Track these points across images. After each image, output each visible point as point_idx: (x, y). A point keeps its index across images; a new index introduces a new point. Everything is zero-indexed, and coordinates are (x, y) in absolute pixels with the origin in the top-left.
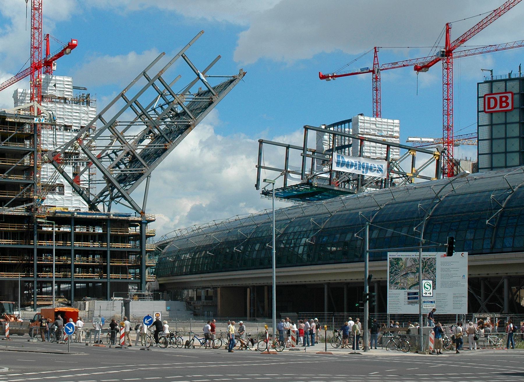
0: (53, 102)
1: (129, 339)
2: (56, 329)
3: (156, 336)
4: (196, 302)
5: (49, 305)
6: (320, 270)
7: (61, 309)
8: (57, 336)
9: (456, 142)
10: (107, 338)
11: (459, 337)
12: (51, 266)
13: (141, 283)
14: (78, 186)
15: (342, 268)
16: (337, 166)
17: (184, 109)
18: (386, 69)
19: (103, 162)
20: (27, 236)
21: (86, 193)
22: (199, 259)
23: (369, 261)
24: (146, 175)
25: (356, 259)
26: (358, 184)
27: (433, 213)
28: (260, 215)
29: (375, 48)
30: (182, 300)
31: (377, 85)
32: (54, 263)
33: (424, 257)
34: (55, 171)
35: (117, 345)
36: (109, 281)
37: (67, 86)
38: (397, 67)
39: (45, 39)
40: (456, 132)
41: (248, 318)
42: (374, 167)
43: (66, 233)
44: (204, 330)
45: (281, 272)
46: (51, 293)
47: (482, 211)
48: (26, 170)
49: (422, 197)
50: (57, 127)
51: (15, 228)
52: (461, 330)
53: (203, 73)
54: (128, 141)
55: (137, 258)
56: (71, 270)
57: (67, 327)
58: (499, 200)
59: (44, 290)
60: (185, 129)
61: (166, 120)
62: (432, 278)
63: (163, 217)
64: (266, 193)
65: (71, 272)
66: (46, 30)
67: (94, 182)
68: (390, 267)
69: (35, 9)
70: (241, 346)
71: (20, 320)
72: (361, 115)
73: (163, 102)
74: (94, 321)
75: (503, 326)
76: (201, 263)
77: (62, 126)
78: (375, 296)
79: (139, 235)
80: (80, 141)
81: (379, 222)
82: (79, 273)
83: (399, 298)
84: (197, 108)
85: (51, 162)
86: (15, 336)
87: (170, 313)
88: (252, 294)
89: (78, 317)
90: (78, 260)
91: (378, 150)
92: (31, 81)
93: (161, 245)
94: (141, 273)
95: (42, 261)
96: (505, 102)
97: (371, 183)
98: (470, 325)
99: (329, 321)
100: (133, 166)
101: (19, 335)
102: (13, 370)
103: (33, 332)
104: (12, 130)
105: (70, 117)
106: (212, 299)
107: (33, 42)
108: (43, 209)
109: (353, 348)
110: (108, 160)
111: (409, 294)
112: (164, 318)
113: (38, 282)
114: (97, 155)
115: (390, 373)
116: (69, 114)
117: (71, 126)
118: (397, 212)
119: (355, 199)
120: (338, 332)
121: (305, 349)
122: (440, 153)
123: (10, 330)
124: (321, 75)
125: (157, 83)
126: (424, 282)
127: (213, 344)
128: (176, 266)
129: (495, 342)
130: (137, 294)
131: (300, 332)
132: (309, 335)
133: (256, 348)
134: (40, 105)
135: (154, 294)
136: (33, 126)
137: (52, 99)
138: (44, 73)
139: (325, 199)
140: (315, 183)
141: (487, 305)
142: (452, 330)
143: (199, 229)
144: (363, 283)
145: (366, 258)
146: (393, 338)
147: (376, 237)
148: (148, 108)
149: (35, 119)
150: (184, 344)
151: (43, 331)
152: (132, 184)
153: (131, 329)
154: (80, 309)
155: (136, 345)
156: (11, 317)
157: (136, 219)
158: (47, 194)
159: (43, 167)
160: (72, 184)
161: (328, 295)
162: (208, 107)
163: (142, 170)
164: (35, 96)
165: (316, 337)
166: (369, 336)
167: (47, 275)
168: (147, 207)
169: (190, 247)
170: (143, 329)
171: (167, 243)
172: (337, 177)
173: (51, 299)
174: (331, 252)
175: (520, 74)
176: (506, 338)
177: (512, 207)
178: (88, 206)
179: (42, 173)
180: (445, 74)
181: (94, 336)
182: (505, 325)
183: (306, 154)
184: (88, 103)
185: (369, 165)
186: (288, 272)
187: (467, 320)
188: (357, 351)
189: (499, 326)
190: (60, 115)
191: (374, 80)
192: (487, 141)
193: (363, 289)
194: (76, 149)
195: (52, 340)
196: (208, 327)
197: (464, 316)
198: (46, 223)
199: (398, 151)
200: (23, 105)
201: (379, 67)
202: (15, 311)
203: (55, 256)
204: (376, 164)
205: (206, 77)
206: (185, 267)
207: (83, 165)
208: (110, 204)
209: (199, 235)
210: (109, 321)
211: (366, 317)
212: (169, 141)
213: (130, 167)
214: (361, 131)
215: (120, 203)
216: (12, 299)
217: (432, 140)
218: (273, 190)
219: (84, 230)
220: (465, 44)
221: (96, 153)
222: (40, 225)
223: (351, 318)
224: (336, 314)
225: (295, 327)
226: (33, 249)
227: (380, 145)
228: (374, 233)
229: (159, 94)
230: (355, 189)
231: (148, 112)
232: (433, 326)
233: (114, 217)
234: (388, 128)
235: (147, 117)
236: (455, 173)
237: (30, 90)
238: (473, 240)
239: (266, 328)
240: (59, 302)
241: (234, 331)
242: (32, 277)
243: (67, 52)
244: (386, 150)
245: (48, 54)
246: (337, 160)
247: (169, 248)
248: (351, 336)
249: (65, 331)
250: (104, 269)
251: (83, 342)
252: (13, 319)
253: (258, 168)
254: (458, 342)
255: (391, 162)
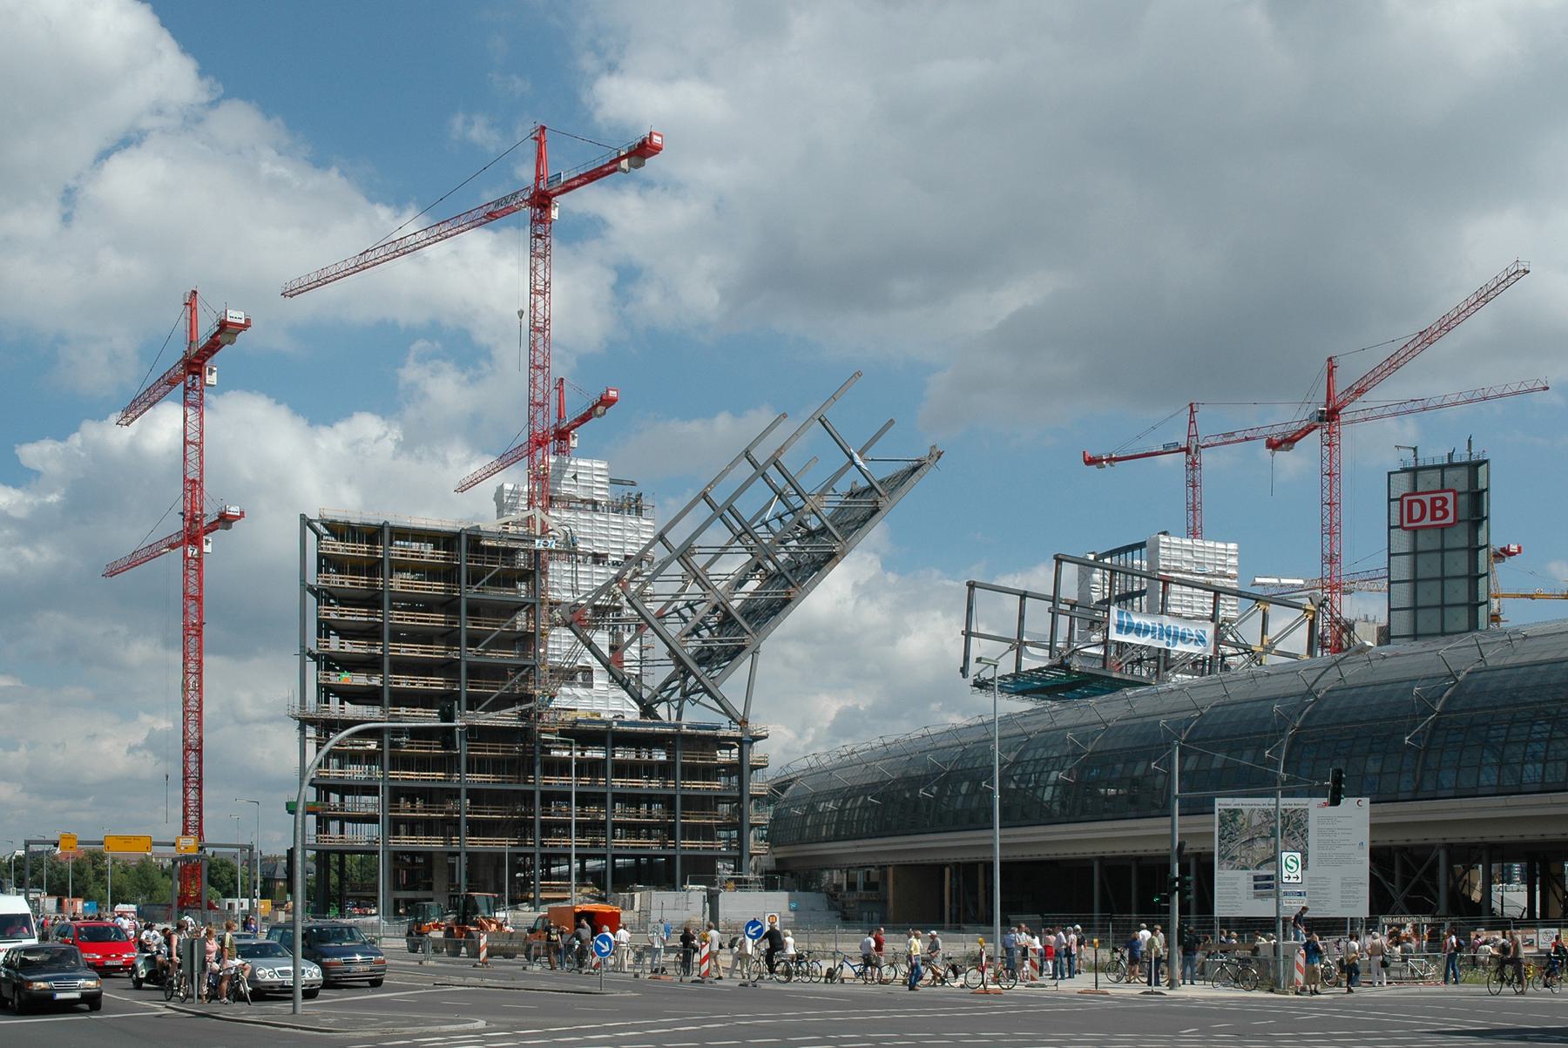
0: (571, 508)
1: (717, 966)
2: (576, 947)
3: (769, 960)
4: (847, 895)
5: (564, 900)
6: (1084, 832)
7: (587, 907)
8: (578, 959)
9: (1346, 586)
10: (676, 963)
11: (1352, 962)
12: (567, 825)
13: (741, 857)
14: (620, 670)
15: (1127, 829)
16: (1117, 632)
17: (822, 522)
18: (1213, 445)
19: (667, 625)
20: (521, 766)
21: (634, 684)
22: (852, 812)
23: (1180, 815)
24: (750, 649)
25: (1155, 811)
26: (1158, 668)
27: (1303, 721)
28: (970, 727)
29: (1191, 405)
30: (819, 890)
31: (1194, 477)
32: (574, 819)
33: (1285, 807)
34: (576, 642)
35: (695, 976)
36: (678, 854)
37: (599, 479)
38: (1233, 442)
39: (555, 388)
40: (1346, 566)
41: (947, 925)
42: (1189, 635)
43: (597, 760)
44: (861, 948)
45: (1009, 836)
46: (568, 877)
47: (1397, 718)
48: (519, 639)
49: (1281, 692)
50: (580, 557)
51: (498, 751)
52: (1357, 948)
53: (860, 454)
54: (715, 583)
55: (734, 810)
56: (606, 832)
57: (598, 942)
58: (1430, 698)
59: (554, 870)
60: (826, 562)
61: (788, 544)
62: (1301, 847)
63: (783, 730)
64: (981, 685)
65: (606, 836)
66: (557, 370)
67: (651, 663)
68: (1220, 827)
69: (538, 330)
70: (934, 978)
71: (508, 928)
72: (1165, 533)
73: (783, 509)
74: (649, 930)
75: (1438, 941)
76: (855, 818)
77: (589, 555)
78: (1192, 883)
79: (737, 764)
80: (623, 583)
81: (1199, 740)
82: (621, 838)
83: (1236, 886)
84: (849, 521)
85: (569, 625)
86: (499, 959)
87: (796, 915)
88: (954, 879)
89: (619, 922)
90: (620, 813)
91: (1197, 602)
92: (529, 468)
93: (779, 783)
94: (740, 838)
95: (550, 815)
96: (1439, 508)
97: (1184, 664)
98: (1375, 938)
99: (1103, 931)
100: (725, 632)
101: (506, 958)
102: (494, 1025)
103: (533, 952)
104: (492, 563)
105: (604, 538)
106: (877, 889)
107: (534, 393)
108: (552, 716)
109: (1149, 983)
110: (678, 620)
111: (1256, 878)
112: (785, 925)
113: (543, 856)
114: (656, 611)
115: (1221, 1031)
116: (603, 532)
117: (605, 556)
118: (1233, 720)
119: (1151, 695)
120: (1120, 952)
121: (1056, 985)
122: (1315, 607)
123: (488, 948)
124: (1086, 457)
125: (772, 471)
126: (1285, 855)
127: (878, 974)
128: (808, 824)
129: (1421, 971)
130: (733, 879)
131: (1047, 953)
132: (1065, 957)
133: (963, 983)
134: (547, 514)
135: (766, 878)
136: (533, 555)
137: (570, 503)
138: (554, 454)
139: (1095, 695)
140: (1076, 664)
141: (1407, 901)
142: (1339, 949)
143: (852, 753)
144: (1168, 857)
145: (1174, 811)
146: (1226, 963)
147: (1193, 769)
148: (754, 519)
149: (537, 541)
150: (824, 974)
151: (552, 950)
152: (724, 667)
153: (721, 947)
154: (623, 908)
155: (731, 977)
156: (490, 922)
157: (732, 734)
158: (560, 686)
159: (552, 633)
160: (607, 666)
161: (1102, 883)
162: (870, 518)
163: (743, 641)
164: (537, 498)
165: (1076, 962)
166: (1179, 958)
167: (560, 842)
168: (752, 711)
169: (836, 787)
170: (745, 946)
171: (791, 780)
172: (1117, 653)
173: (567, 889)
174: (1107, 798)
175: (1471, 454)
176: (1442, 964)
177: (1455, 712)
178: (638, 709)
179: (550, 646)
180: (1326, 454)
181: (650, 959)
182: (1441, 938)
183: (1059, 609)
184: (639, 511)
185: (1180, 631)
186: (1025, 835)
187: (1367, 928)
188: (1156, 989)
189: (1429, 941)
190: (585, 534)
191: (1190, 467)
192: (1407, 584)
193: (1167, 868)
194: (615, 599)
195: (571, 968)
196: (870, 942)
197: (1362, 921)
198: (557, 743)
199: (1234, 603)
200: (513, 514)
201: (1198, 441)
202: (498, 911)
203: (576, 805)
204: (1193, 629)
205: (865, 461)
206: (825, 826)
207: (629, 630)
208: (681, 704)
209: (851, 764)
210: (680, 931)
211: (1174, 923)
212: (795, 584)
213: (719, 634)
214: (1165, 565)
215: (700, 703)
216: (493, 888)
217: (1301, 582)
218: (994, 678)
219: (632, 756)
220: (1364, 396)
221: (654, 607)
222: (547, 746)
223: (1144, 925)
224: (1116, 916)
225: (1036, 943)
226: (533, 793)
227: (1201, 591)
228: (1189, 760)
229: (776, 493)
230: (1153, 676)
231: (755, 528)
232: (1302, 940)
233: (689, 731)
234: (1216, 560)
235: (752, 538)
236: (1345, 646)
237: (527, 486)
238: (1381, 774)
239: (981, 943)
240: (583, 894)
241: (919, 950)
242: (531, 845)
243: (599, 413)
244: (1212, 601)
245: (563, 416)
246: (1119, 621)
247: (794, 789)
248: (1145, 960)
249: (594, 950)
250: (670, 831)
251: (630, 970)
252: (494, 926)
253: (966, 636)
254: (1350, 971)
255: (1222, 625)
